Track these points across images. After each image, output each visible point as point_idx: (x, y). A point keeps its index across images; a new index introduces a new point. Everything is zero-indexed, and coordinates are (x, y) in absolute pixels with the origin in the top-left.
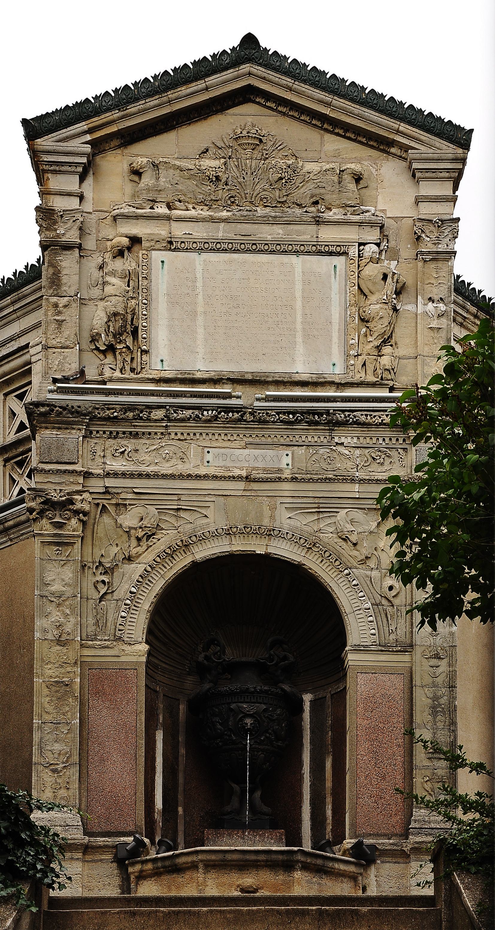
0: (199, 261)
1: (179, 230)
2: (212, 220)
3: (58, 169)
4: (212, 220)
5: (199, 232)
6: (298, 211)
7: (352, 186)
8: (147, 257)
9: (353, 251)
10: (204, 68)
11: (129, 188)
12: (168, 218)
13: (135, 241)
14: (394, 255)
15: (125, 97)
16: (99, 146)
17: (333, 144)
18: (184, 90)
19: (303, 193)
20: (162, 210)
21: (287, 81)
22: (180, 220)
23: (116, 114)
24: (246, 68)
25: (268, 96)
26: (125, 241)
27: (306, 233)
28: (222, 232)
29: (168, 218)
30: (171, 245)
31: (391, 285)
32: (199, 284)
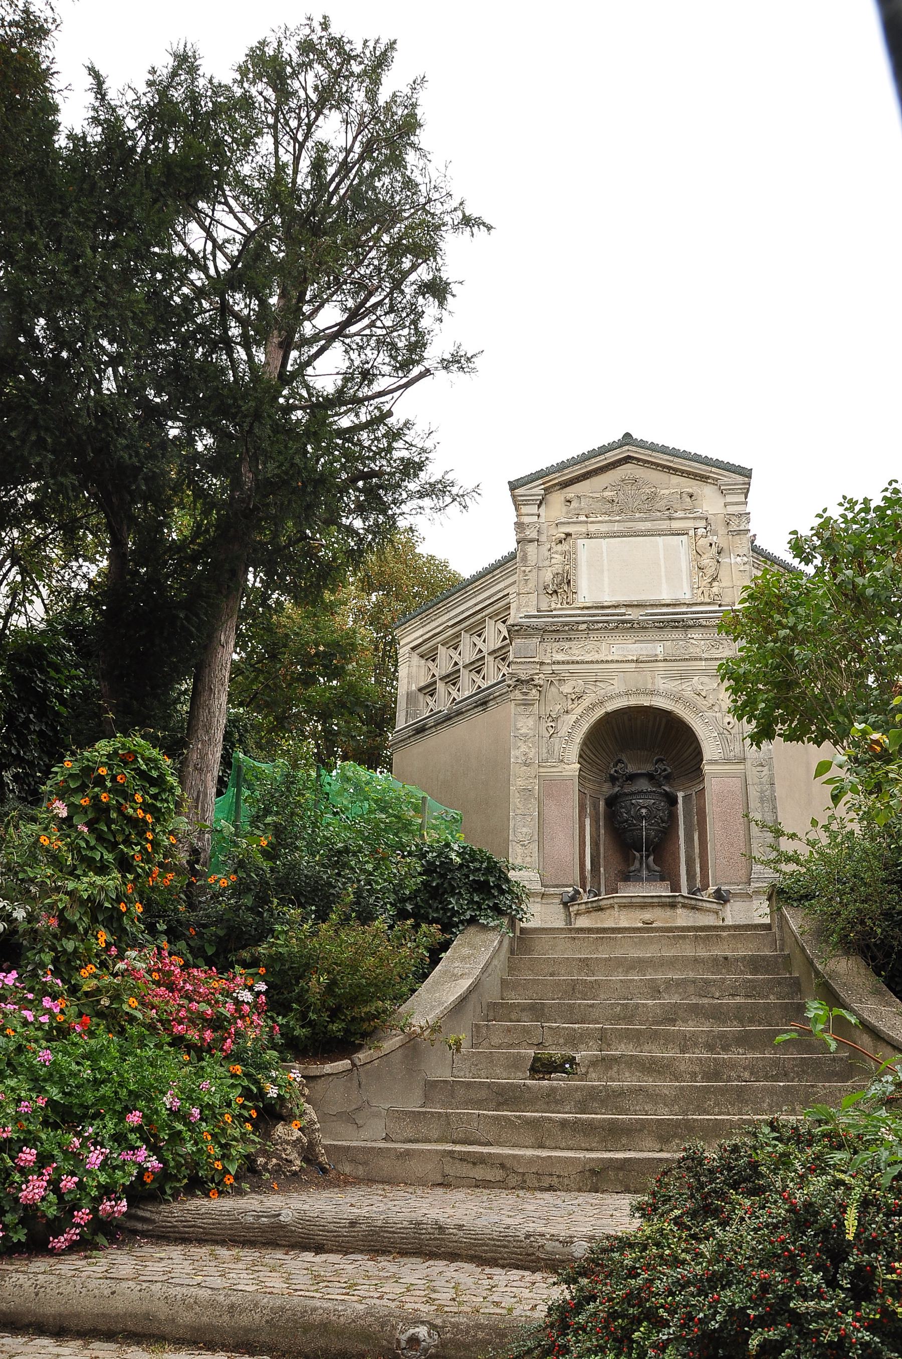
1: (592, 528)
2: (611, 521)
3: (526, 503)
4: (611, 521)
5: (604, 528)
6: (659, 514)
7: (688, 499)
8: (575, 544)
9: (691, 533)
10: (603, 450)
11: (564, 509)
12: (587, 522)
13: (568, 535)
14: (715, 533)
15: (562, 466)
17: (676, 480)
18: (593, 460)
21: (650, 452)
22: (592, 522)
23: (558, 475)
24: (626, 448)
25: (638, 460)
26: (563, 536)
27: (665, 525)
28: (616, 527)
29: (587, 522)
30: (588, 536)
31: (714, 549)
32: (605, 554)
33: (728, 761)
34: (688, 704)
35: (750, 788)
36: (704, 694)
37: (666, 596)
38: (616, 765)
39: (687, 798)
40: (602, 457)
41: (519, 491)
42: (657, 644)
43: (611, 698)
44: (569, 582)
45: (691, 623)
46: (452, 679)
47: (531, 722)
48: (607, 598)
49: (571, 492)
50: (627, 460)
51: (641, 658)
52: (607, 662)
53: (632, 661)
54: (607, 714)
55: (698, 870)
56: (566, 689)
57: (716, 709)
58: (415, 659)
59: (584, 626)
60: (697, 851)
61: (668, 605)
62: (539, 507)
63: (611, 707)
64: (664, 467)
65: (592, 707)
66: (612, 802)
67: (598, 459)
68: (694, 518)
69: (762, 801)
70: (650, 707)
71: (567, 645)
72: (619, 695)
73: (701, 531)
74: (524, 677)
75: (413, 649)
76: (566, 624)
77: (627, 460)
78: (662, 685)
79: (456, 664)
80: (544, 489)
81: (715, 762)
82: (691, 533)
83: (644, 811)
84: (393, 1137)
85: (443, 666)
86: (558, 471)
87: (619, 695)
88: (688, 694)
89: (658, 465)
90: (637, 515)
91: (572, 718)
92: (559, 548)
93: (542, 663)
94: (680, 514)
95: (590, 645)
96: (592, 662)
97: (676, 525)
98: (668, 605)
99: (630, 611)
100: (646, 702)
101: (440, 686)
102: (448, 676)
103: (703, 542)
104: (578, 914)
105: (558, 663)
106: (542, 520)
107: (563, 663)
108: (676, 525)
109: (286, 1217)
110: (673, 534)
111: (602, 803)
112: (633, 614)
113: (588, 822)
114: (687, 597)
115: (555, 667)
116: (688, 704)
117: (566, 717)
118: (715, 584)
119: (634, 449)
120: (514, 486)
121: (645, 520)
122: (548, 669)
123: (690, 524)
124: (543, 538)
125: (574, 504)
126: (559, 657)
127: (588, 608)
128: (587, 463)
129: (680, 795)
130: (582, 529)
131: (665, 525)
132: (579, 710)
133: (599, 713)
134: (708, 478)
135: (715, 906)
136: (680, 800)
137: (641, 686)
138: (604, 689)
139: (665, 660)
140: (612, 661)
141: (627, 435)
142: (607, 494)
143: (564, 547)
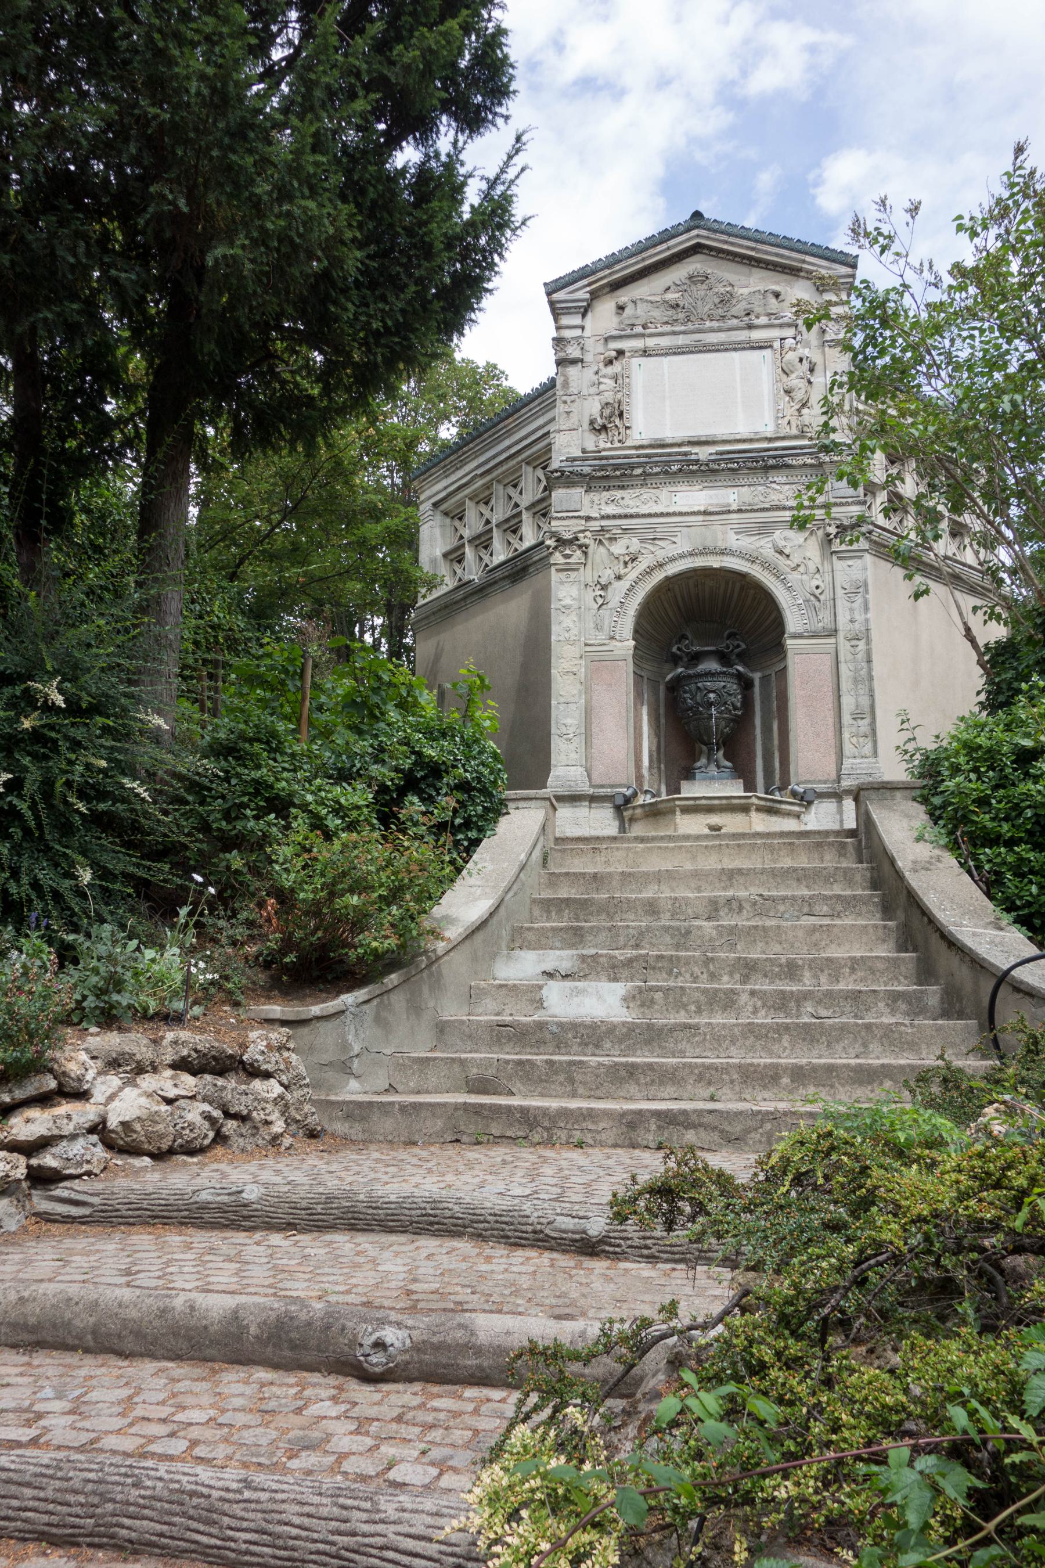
0: (666, 360)
1: (651, 342)
2: (674, 333)
3: (569, 311)
4: (674, 333)
5: (665, 342)
6: (735, 322)
7: (774, 300)
9: (777, 344)
10: (666, 236)
12: (643, 335)
13: (620, 353)
15: (612, 261)
16: (595, 295)
19: (739, 309)
20: (639, 329)
21: (725, 237)
22: (651, 335)
24: (695, 232)
25: (711, 248)
27: (743, 335)
28: (681, 340)
30: (645, 353)
31: (806, 365)
33: (815, 635)
34: (766, 565)
35: (843, 667)
36: (787, 551)
37: (742, 427)
38: (679, 641)
39: (765, 679)
40: (664, 246)
41: (556, 296)
42: (731, 490)
43: (672, 560)
44: (621, 415)
45: (771, 462)
46: (482, 541)
47: (574, 591)
48: (669, 434)
49: (624, 296)
50: (696, 249)
51: (711, 509)
52: (668, 514)
53: (699, 513)
54: (667, 579)
55: (777, 765)
56: (618, 548)
57: (802, 569)
58: (439, 517)
59: (639, 471)
60: (776, 742)
61: (744, 441)
62: (584, 315)
63: (672, 569)
64: (744, 257)
65: (649, 571)
66: (674, 687)
67: (659, 248)
68: (781, 326)
69: (856, 681)
70: (721, 570)
71: (618, 494)
72: (682, 556)
73: (790, 342)
74: (567, 536)
75: (436, 505)
76: (616, 467)
77: (696, 249)
78: (734, 541)
79: (488, 522)
80: (591, 293)
81: (800, 636)
82: (777, 344)
83: (712, 696)
84: (400, 1088)
85: (473, 525)
86: (608, 267)
87: (682, 556)
88: (769, 553)
89: (735, 255)
90: (708, 324)
91: (625, 584)
92: (610, 370)
93: (588, 518)
94: (763, 320)
95: (647, 493)
96: (650, 515)
97: (757, 335)
98: (744, 441)
99: (695, 450)
100: (715, 562)
101: (469, 552)
102: (479, 537)
103: (791, 356)
104: (632, 820)
105: (608, 517)
106: (587, 333)
107: (614, 517)
108: (757, 335)
109: (252, 1193)
110: (753, 348)
111: (662, 688)
112: (703, 453)
113: (645, 711)
114: (770, 431)
115: (604, 523)
116: (766, 565)
117: (617, 584)
118: (805, 411)
119: (704, 233)
120: (552, 288)
121: (720, 330)
122: (595, 525)
123: (776, 333)
124: (588, 358)
125: (629, 311)
126: (610, 510)
127: (642, 447)
128: (644, 255)
129: (757, 676)
130: (638, 344)
131: (743, 335)
132: (633, 575)
133: (659, 576)
134: (800, 270)
135: (796, 808)
136: (757, 683)
137: (709, 543)
138: (665, 550)
139: (740, 511)
140: (674, 514)
141: (697, 215)
142: (670, 296)
143: (617, 367)
